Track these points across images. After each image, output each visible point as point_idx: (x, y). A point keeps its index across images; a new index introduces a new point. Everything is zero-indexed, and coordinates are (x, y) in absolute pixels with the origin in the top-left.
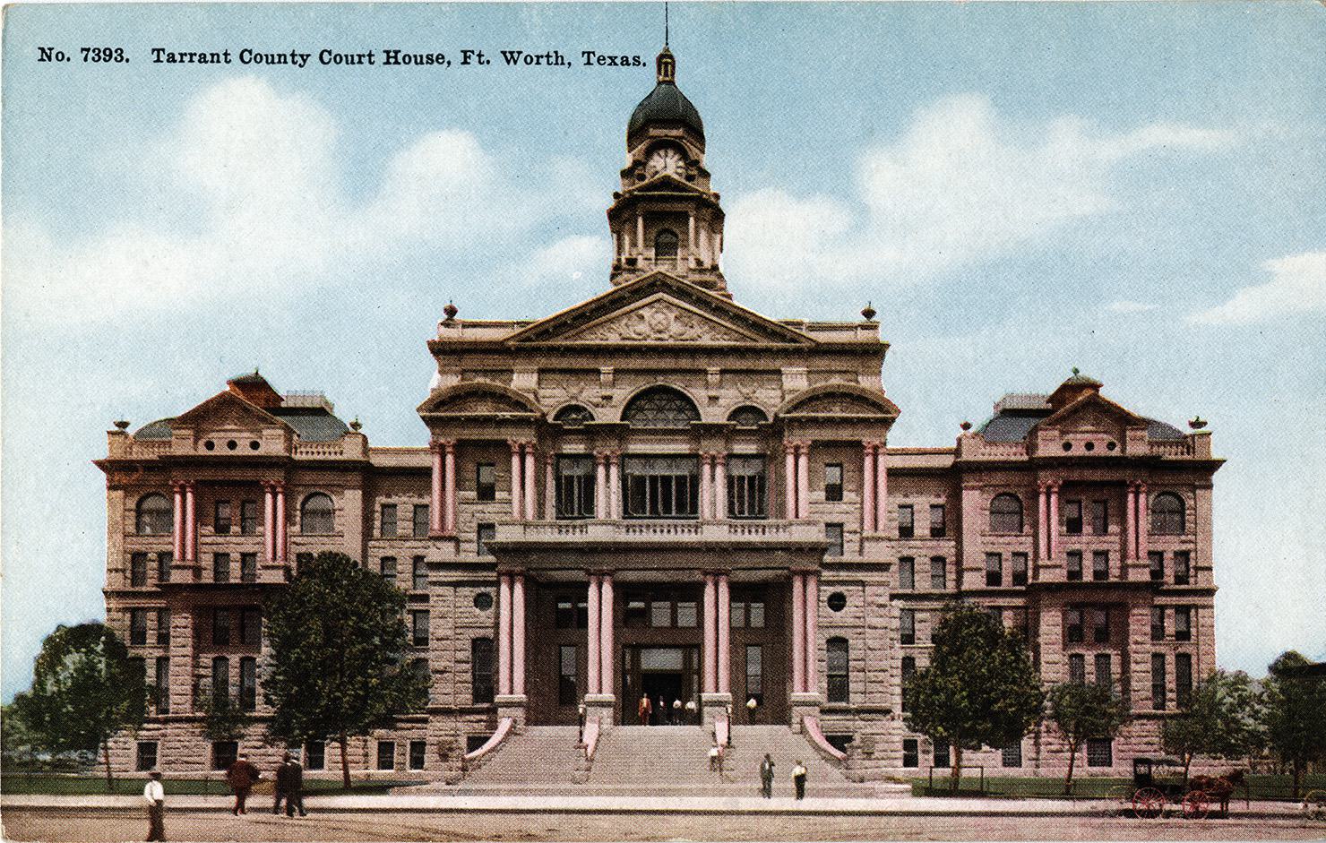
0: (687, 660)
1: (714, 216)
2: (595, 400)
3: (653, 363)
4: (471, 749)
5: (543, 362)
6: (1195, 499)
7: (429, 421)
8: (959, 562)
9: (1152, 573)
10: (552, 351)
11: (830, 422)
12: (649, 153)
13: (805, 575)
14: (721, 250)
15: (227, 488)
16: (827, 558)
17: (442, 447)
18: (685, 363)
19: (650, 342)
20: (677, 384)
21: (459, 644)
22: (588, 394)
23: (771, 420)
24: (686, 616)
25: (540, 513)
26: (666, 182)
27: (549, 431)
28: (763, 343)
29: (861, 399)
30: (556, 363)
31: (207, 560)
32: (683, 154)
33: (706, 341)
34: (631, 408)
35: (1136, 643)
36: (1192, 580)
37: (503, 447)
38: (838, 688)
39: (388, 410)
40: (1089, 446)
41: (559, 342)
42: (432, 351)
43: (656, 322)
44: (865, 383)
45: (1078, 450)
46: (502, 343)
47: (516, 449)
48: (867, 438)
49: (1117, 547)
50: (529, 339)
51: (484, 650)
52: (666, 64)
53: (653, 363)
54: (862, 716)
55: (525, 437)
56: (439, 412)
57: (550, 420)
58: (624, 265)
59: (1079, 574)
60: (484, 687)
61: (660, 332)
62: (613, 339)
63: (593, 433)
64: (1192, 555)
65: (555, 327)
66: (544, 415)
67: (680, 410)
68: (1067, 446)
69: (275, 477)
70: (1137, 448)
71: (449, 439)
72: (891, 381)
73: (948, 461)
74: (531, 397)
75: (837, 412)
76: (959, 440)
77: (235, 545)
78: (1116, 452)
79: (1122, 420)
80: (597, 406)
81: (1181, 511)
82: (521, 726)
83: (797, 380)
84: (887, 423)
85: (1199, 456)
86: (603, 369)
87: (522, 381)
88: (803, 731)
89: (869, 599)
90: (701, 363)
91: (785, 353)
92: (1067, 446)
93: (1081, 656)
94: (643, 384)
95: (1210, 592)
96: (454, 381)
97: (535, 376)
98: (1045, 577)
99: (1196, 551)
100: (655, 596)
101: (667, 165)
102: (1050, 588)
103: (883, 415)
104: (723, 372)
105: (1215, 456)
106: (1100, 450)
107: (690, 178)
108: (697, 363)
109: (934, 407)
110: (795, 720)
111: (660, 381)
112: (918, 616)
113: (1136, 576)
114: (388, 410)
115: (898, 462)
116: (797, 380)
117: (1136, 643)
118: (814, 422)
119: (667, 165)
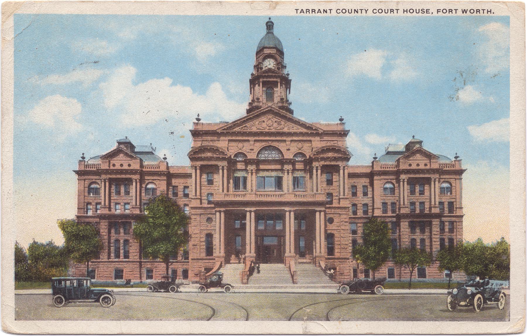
0: (279, 241)
1: (286, 82)
2: (248, 151)
4: (206, 273)
5: (230, 138)
7: (192, 159)
8: (373, 206)
9: (440, 209)
12: (264, 59)
13: (320, 211)
14: (289, 93)
15: (119, 181)
16: (327, 206)
17: (196, 167)
18: (278, 138)
19: (266, 130)
20: (275, 144)
21: (202, 236)
22: (246, 148)
23: (308, 157)
26: (270, 70)
27: (232, 163)
32: (276, 60)
35: (435, 235)
36: (454, 212)
37: (216, 167)
38: (331, 251)
39: (176, 155)
40: (418, 165)
43: (268, 123)
44: (340, 144)
45: (414, 167)
46: (216, 131)
48: (340, 164)
49: (428, 200)
51: (209, 236)
52: (270, 25)
53: (267, 138)
55: (225, 163)
57: (232, 157)
58: (256, 100)
59: (415, 210)
60: (209, 251)
62: (254, 129)
63: (248, 162)
64: (455, 203)
66: (230, 156)
69: (137, 177)
70: (435, 166)
73: (368, 171)
76: (373, 163)
78: (428, 167)
79: (429, 156)
83: (318, 143)
84: (348, 159)
85: (457, 168)
87: (222, 143)
91: (312, 135)
92: (410, 165)
94: (264, 144)
95: (462, 216)
96: (199, 144)
97: (227, 142)
98: (403, 211)
99: (456, 202)
101: (270, 64)
102: (405, 216)
103: (346, 157)
106: (422, 167)
107: (278, 69)
109: (364, 149)
111: (270, 143)
113: (434, 211)
114: (176, 155)
115: (351, 171)
116: (318, 143)
117: (435, 235)
118: (323, 159)
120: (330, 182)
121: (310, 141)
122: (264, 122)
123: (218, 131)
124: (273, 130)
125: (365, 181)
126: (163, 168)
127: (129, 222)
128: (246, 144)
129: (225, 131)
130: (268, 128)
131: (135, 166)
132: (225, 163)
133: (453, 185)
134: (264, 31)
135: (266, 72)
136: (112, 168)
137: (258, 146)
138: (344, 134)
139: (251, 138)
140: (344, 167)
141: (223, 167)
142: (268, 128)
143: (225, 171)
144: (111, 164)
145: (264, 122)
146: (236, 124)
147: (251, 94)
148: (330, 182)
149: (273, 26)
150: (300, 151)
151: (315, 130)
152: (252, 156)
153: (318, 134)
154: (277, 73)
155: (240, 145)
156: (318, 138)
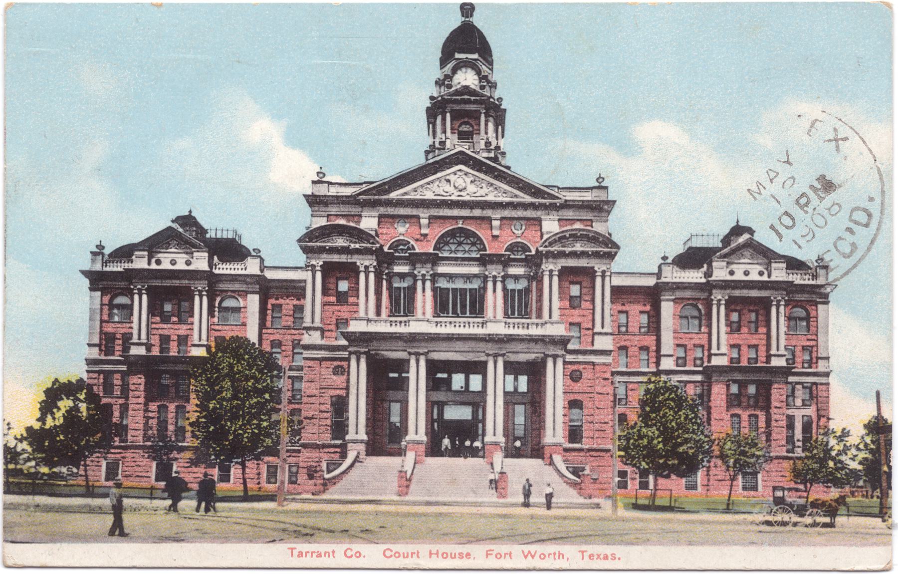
0: (475, 413)
1: (497, 113)
3: (456, 212)
4: (329, 471)
5: (382, 210)
7: (306, 250)
9: (787, 360)
12: (454, 71)
13: (555, 357)
14: (503, 137)
15: (170, 295)
16: (570, 347)
18: (477, 212)
19: (453, 198)
23: (533, 253)
24: (476, 382)
25: (378, 313)
26: (466, 90)
27: (385, 260)
28: (528, 199)
29: (595, 238)
30: (391, 211)
31: (155, 340)
32: (478, 72)
33: (491, 198)
34: (442, 242)
35: (776, 407)
36: (814, 365)
38: (574, 434)
40: (746, 273)
41: (394, 195)
44: (599, 227)
45: (739, 276)
47: (362, 269)
48: (599, 266)
49: (764, 342)
53: (456, 212)
54: (591, 453)
55: (369, 261)
56: (311, 242)
57: (386, 249)
58: (437, 145)
59: (739, 360)
60: (339, 428)
61: (460, 191)
62: (429, 195)
63: (414, 259)
66: (382, 246)
67: (473, 244)
68: (732, 273)
69: (201, 285)
71: (318, 262)
72: (613, 226)
73: (651, 282)
75: (578, 247)
76: (660, 267)
77: (173, 330)
78: (765, 278)
79: (767, 255)
80: (417, 240)
81: (807, 318)
82: (363, 456)
83: (551, 225)
84: (611, 256)
86: (421, 215)
87: (369, 222)
88: (552, 463)
90: (488, 213)
93: (738, 416)
95: (827, 375)
96: (322, 222)
98: (715, 361)
99: (817, 346)
101: (467, 78)
102: (720, 370)
104: (502, 219)
106: (754, 276)
107: (483, 87)
108: (485, 212)
109: (645, 242)
110: (547, 455)
112: (630, 386)
113: (776, 362)
115: (618, 281)
116: (551, 225)
117: (776, 407)
118: (562, 255)
124: (467, 198)
127: (184, 375)
132: (369, 261)
133: (813, 314)
135: (457, 92)
153: (553, 207)
154: (478, 95)
156: (555, 216)
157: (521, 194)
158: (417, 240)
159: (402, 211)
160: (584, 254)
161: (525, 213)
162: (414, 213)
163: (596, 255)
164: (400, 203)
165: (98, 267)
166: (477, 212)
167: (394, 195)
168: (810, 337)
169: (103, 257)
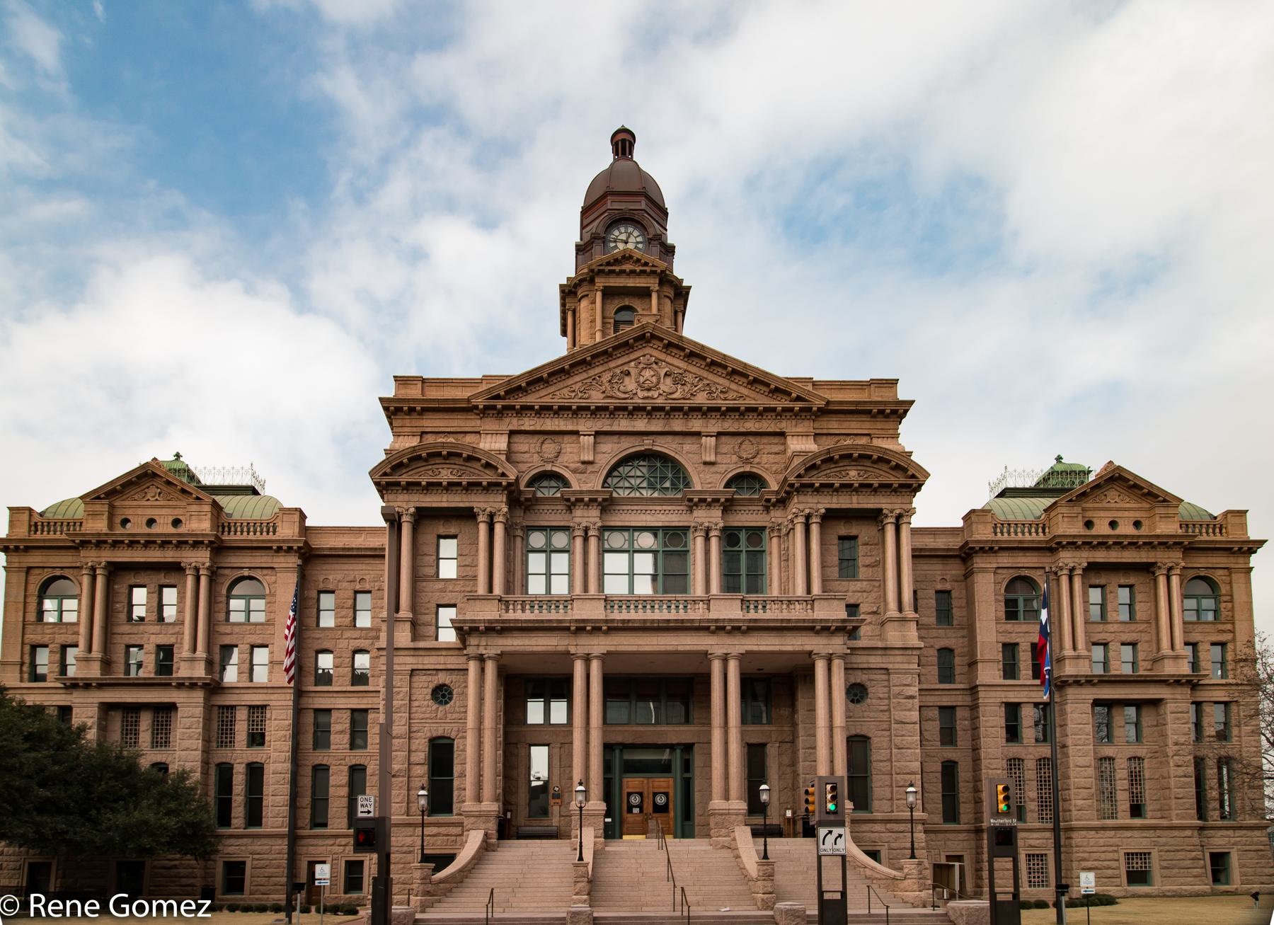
2: (573, 466)
3: (640, 425)
5: (514, 423)
6: (1230, 583)
10: (527, 408)
11: (846, 487)
18: (678, 425)
19: (636, 400)
20: (665, 446)
22: (569, 457)
26: (627, 257)
28: (762, 401)
29: (883, 460)
30: (528, 424)
40: (1113, 524)
41: (530, 399)
42: (386, 409)
45: (1102, 528)
46: (468, 400)
50: (498, 397)
52: (624, 141)
53: (640, 425)
56: (390, 477)
61: (649, 390)
65: (529, 384)
68: (1089, 524)
69: (202, 557)
71: (407, 504)
72: (912, 437)
73: (955, 543)
74: (503, 458)
75: (853, 475)
83: (802, 444)
85: (1233, 535)
87: (493, 443)
89: (895, 690)
90: (696, 424)
92: (1089, 524)
97: (505, 439)
100: (658, 688)
101: (627, 240)
105: (1253, 535)
108: (690, 424)
111: (647, 444)
119: (627, 240)
120: (848, 567)
121: (782, 434)
122: (628, 374)
123: (474, 402)
125: (955, 569)
126: (288, 531)
128: (568, 446)
129: (499, 404)
130: (641, 394)
131: (200, 524)
132: (498, 503)
134: (606, 158)
136: (119, 530)
137: (611, 451)
138: (898, 411)
139: (586, 425)
140: (899, 517)
141: (491, 516)
142: (641, 394)
143: (499, 529)
144: (118, 520)
145: (628, 374)
146: (537, 379)
147: (564, 333)
148: (848, 567)
149: (632, 145)
150: (747, 468)
151: (799, 399)
152: (591, 483)
155: (550, 448)
157: (753, 394)
158: (574, 471)
159: (550, 424)
160: (865, 487)
161: (757, 425)
162: (570, 428)
163: (885, 487)
164: (545, 410)
165: (22, 532)
166: (678, 425)
167: (530, 399)
168: (1221, 627)
169: (31, 515)
